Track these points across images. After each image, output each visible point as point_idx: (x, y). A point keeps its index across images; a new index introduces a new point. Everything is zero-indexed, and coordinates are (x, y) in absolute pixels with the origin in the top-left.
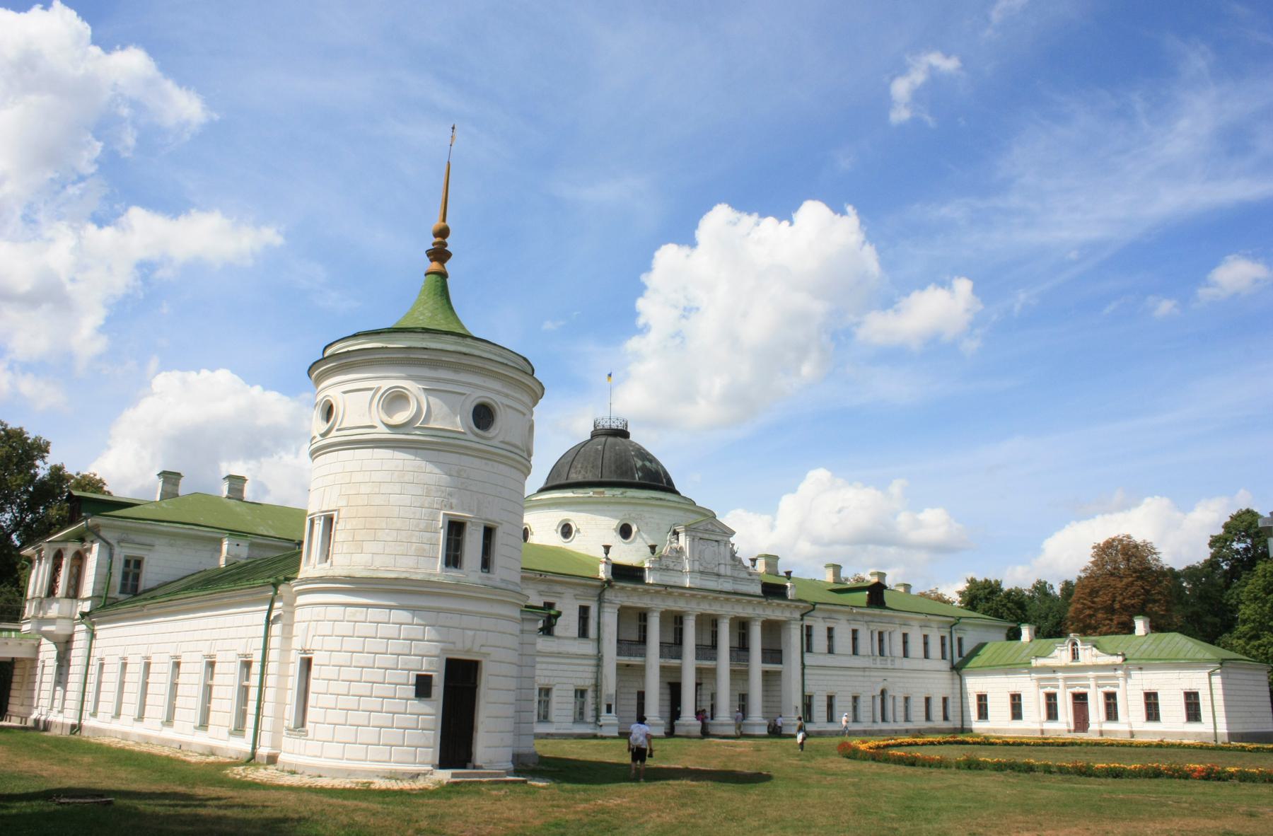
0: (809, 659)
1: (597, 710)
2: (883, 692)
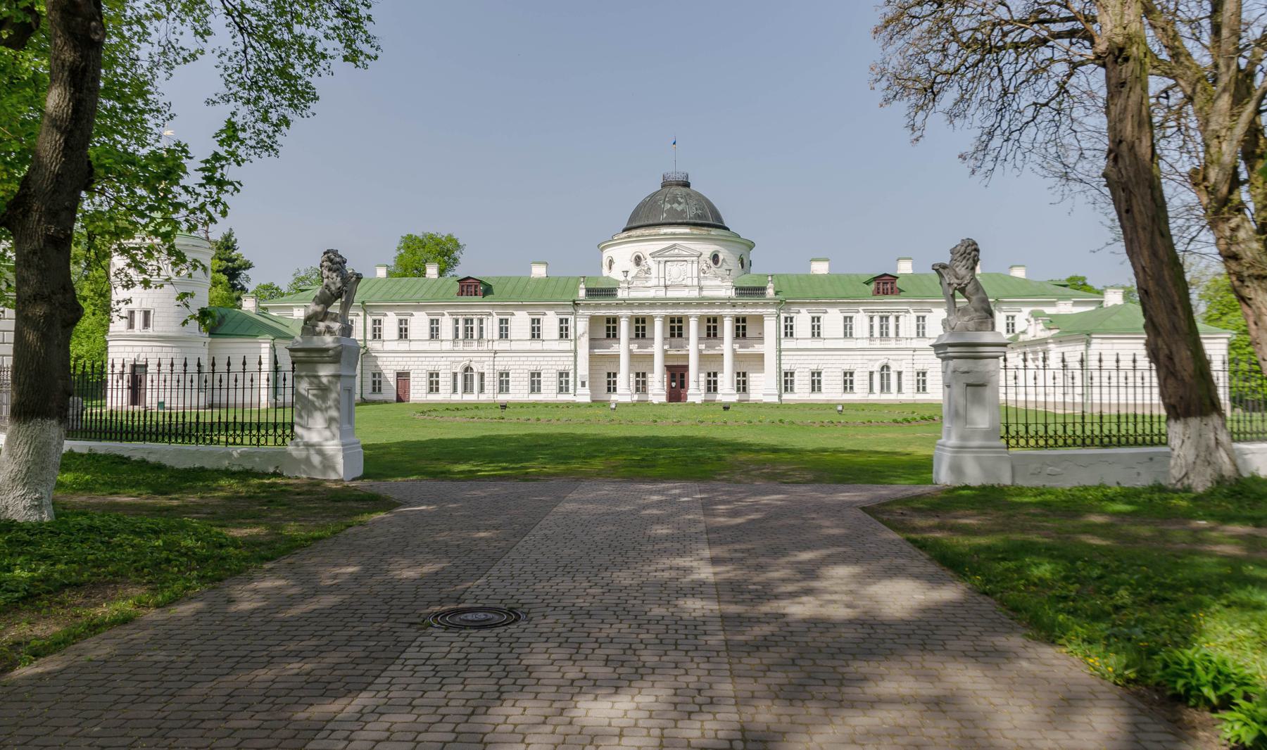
0: (786, 344)
1: (575, 385)
2: (885, 367)
